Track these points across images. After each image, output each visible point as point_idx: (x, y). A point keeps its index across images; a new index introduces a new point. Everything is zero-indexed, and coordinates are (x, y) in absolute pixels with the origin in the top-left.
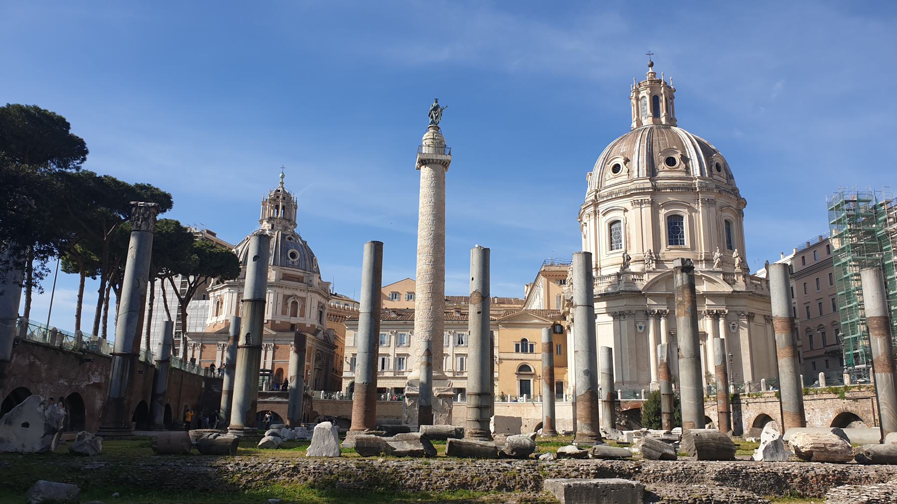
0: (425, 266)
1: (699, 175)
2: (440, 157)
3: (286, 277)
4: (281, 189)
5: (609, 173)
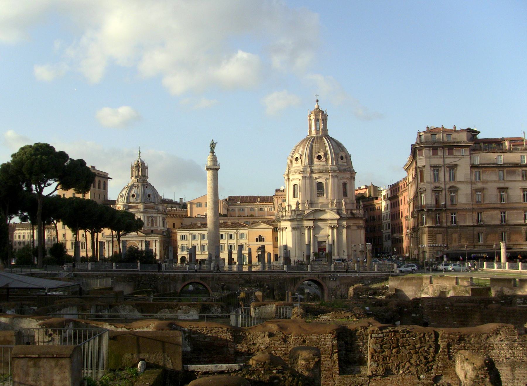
0: (211, 215)
1: (331, 164)
2: (215, 167)
3: (146, 208)
4: (139, 160)
5: (294, 161)
